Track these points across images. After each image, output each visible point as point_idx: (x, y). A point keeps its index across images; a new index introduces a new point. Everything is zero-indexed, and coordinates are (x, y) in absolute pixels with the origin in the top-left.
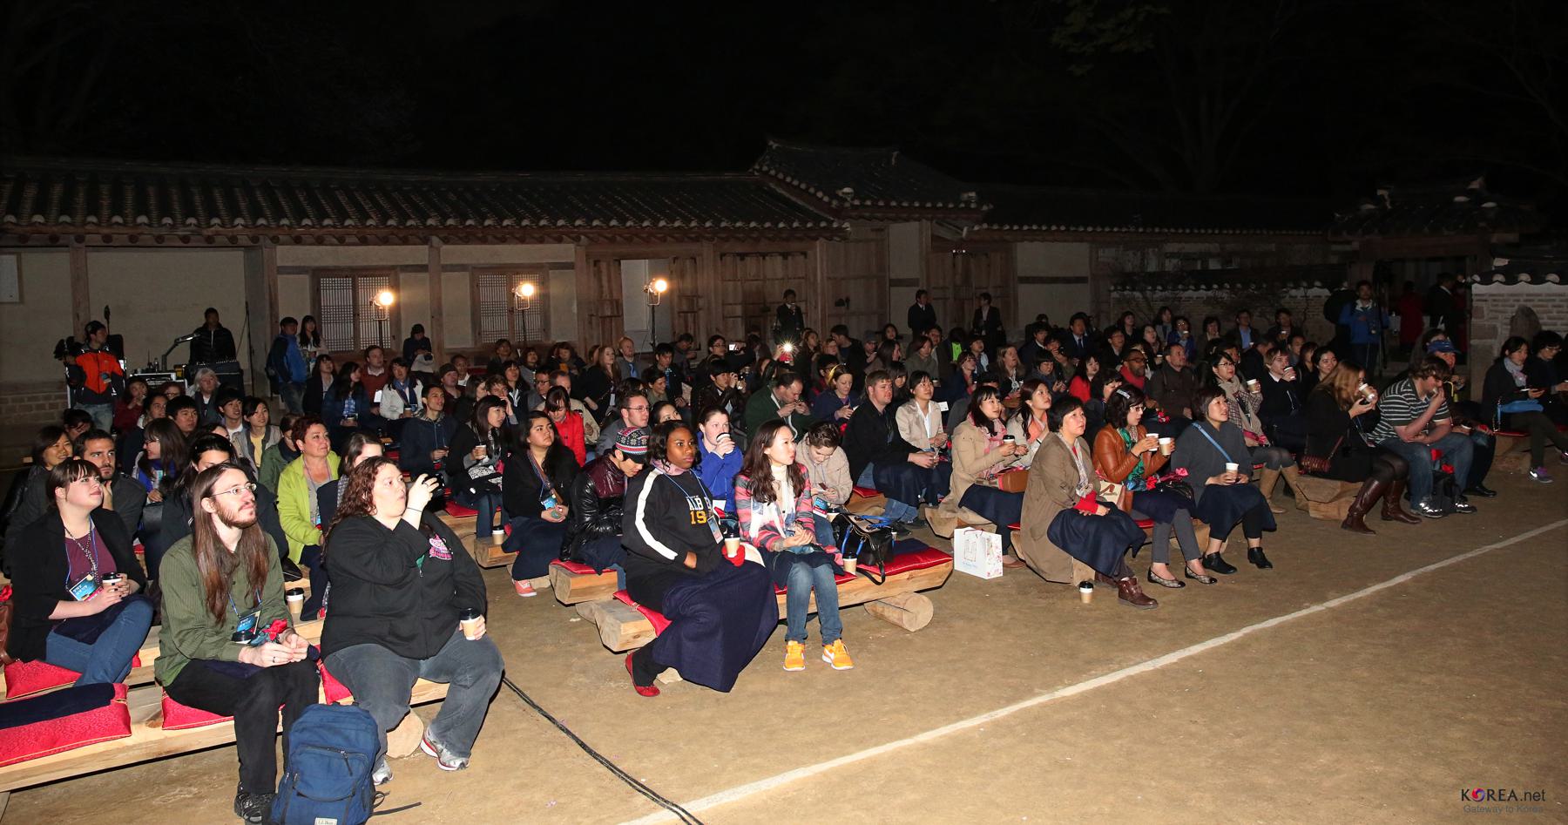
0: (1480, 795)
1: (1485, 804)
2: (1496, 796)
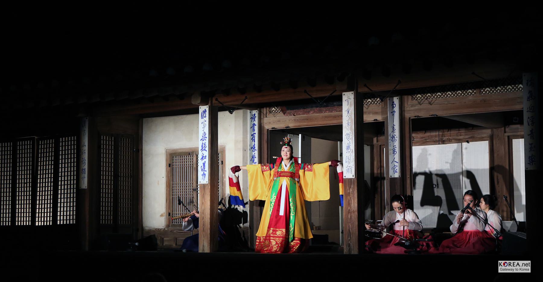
0: (506, 264)
1: (508, 267)
2: (512, 265)
